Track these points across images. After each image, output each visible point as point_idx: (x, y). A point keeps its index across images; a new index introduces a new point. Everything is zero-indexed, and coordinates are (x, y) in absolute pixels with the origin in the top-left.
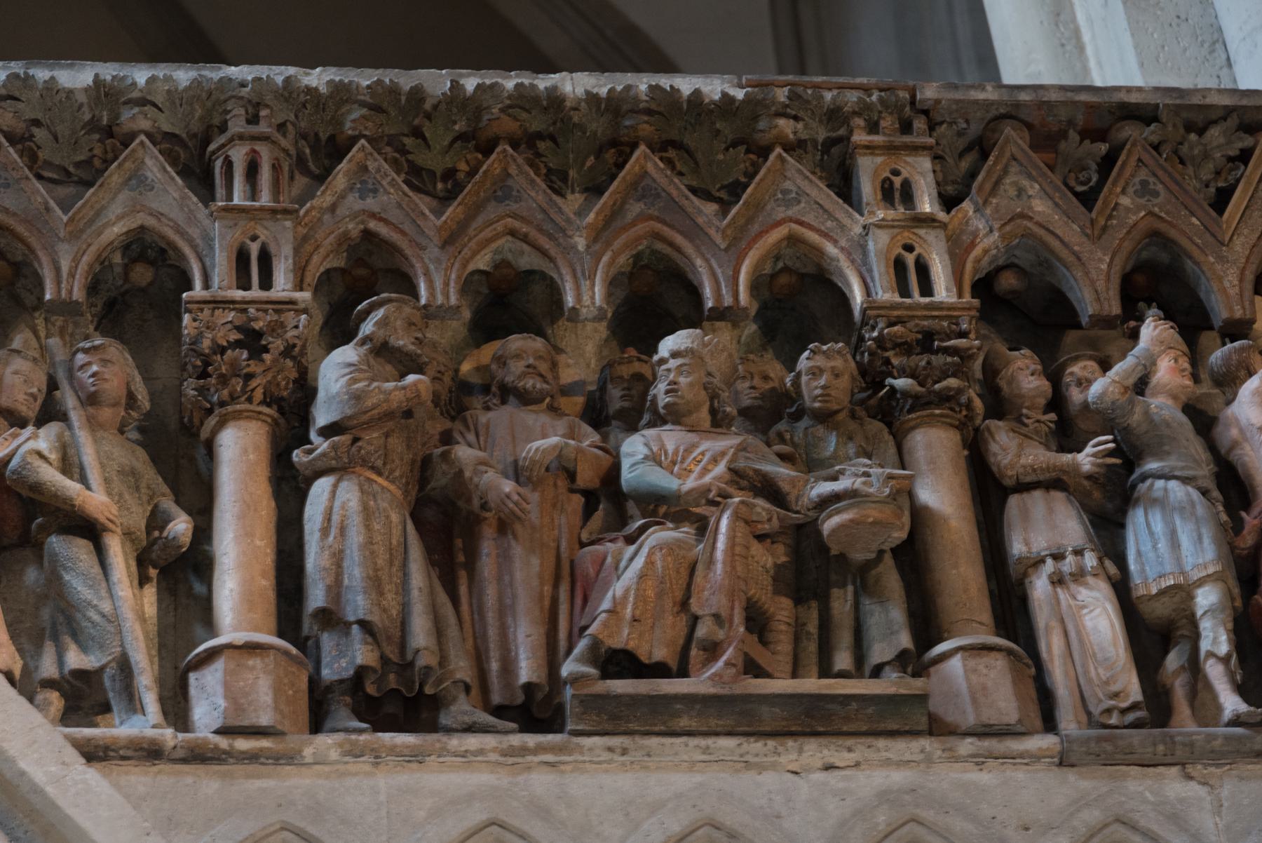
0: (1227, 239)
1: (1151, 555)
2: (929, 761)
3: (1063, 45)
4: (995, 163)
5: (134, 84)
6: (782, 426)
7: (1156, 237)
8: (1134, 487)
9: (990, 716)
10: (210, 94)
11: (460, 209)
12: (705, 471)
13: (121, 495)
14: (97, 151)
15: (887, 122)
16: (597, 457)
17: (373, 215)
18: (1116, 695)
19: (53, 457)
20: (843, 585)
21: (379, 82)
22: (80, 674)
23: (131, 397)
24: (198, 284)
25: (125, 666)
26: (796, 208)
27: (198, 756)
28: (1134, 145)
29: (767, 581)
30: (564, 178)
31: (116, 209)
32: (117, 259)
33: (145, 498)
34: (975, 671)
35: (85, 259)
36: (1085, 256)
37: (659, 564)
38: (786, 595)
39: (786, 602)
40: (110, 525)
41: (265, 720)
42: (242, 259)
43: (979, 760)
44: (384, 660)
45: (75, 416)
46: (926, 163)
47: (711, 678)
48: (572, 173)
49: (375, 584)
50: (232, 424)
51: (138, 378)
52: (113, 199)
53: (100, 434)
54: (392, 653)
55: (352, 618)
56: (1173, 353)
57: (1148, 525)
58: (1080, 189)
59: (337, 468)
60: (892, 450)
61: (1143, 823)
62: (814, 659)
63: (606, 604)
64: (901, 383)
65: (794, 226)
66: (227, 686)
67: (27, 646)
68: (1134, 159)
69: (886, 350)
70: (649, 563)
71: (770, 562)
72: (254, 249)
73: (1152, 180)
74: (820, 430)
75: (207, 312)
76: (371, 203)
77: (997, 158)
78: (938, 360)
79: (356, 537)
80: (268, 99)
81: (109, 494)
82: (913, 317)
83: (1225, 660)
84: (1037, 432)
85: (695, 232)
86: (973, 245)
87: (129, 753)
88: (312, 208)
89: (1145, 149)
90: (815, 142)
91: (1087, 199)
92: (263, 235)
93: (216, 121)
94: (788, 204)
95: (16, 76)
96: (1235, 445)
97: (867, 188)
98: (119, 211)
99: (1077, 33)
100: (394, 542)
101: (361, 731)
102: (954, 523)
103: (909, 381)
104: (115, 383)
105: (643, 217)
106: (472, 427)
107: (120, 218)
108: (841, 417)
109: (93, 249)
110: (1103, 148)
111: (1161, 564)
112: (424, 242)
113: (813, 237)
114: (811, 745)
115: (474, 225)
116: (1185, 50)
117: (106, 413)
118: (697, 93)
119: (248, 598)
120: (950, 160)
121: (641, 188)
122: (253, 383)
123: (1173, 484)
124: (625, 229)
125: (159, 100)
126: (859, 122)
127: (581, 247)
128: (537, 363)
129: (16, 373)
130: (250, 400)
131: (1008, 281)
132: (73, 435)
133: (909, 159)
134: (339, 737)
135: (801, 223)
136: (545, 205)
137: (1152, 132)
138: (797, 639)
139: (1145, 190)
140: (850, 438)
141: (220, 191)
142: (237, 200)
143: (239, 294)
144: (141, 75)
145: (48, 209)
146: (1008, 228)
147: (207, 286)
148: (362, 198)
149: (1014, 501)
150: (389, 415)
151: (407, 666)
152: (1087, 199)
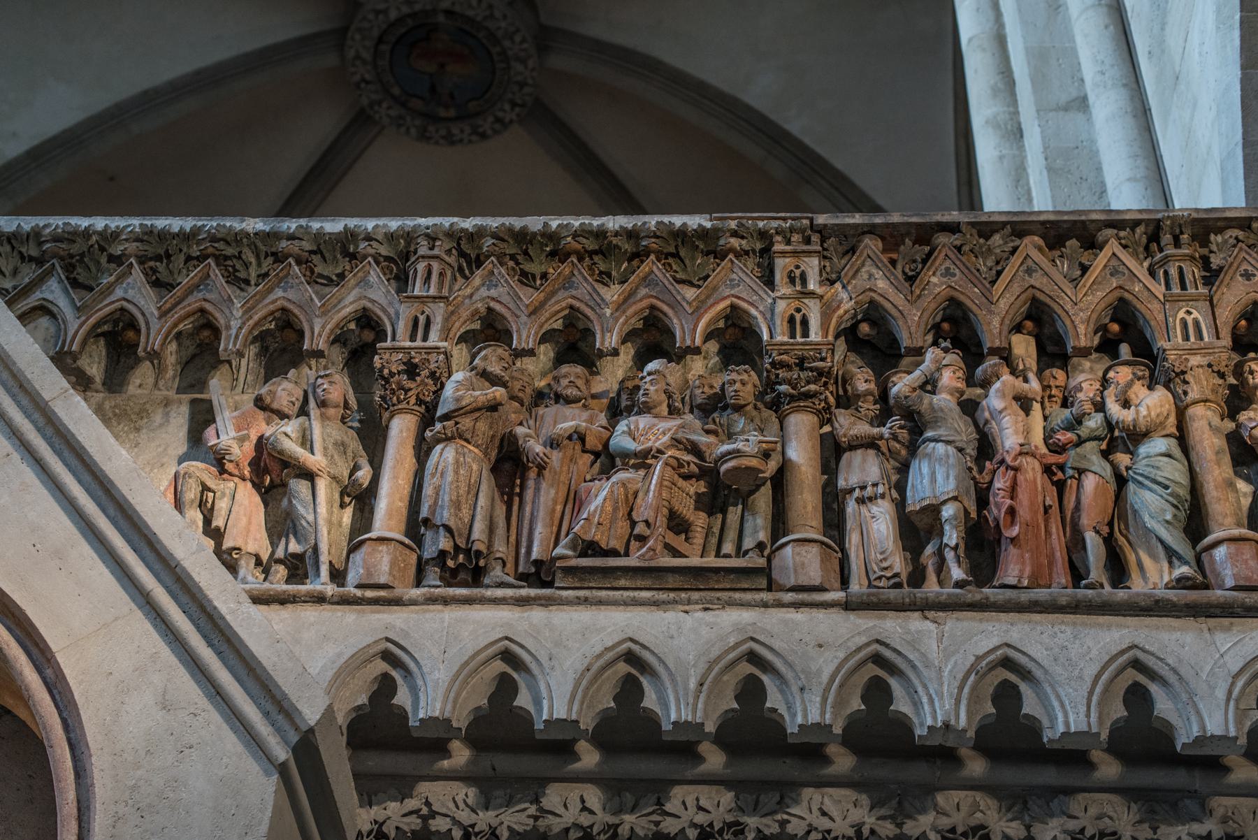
0: (995, 300)
1: (919, 486)
2: (765, 605)
3: (1019, 199)
4: (857, 260)
5: (366, 229)
6: (715, 415)
7: (953, 301)
9: (803, 581)
10: (408, 233)
11: (542, 294)
12: (658, 439)
13: (332, 457)
15: (796, 238)
16: (600, 432)
17: (493, 299)
18: (886, 569)
22: (294, 556)
23: (346, 402)
24: (389, 339)
26: (736, 289)
28: (944, 246)
29: (691, 503)
30: (609, 275)
31: (350, 298)
32: (352, 326)
33: (350, 458)
35: (329, 327)
36: (905, 313)
37: (616, 492)
39: (703, 515)
40: (321, 473)
41: (383, 580)
43: (797, 605)
44: (456, 547)
46: (815, 261)
48: (614, 273)
49: (457, 505)
51: (351, 391)
55: (439, 523)
56: (952, 368)
57: (920, 469)
58: (910, 274)
60: (776, 426)
61: (893, 644)
62: (714, 547)
64: (783, 388)
65: (733, 299)
68: (943, 254)
69: (778, 369)
71: (692, 491)
72: (422, 319)
73: (952, 267)
74: (736, 416)
75: (388, 355)
76: (493, 293)
78: (804, 375)
79: (450, 477)
81: (325, 455)
83: (956, 548)
84: (866, 415)
86: (839, 307)
87: (308, 599)
88: (459, 296)
89: (950, 249)
90: (754, 251)
91: (911, 279)
92: (427, 311)
93: (412, 249)
94: (733, 287)
95: (301, 226)
96: (987, 422)
97: (779, 276)
99: (1029, 192)
100: (472, 481)
102: (803, 469)
103: (787, 387)
104: (336, 394)
106: (533, 416)
107: (351, 303)
108: (749, 408)
110: (927, 249)
111: (924, 492)
112: (518, 313)
114: (695, 596)
116: (1083, 198)
117: (331, 411)
118: (684, 224)
119: (390, 514)
120: (835, 260)
122: (410, 394)
125: (380, 238)
126: (779, 238)
127: (608, 315)
128: (576, 381)
129: (284, 390)
130: (408, 403)
132: (310, 424)
133: (805, 259)
136: (591, 291)
137: (955, 239)
139: (948, 272)
140: (752, 421)
141: (410, 288)
142: (416, 293)
144: (370, 224)
145: (312, 299)
146: (860, 297)
147: (394, 339)
149: (846, 456)
151: (468, 551)
152: (911, 279)
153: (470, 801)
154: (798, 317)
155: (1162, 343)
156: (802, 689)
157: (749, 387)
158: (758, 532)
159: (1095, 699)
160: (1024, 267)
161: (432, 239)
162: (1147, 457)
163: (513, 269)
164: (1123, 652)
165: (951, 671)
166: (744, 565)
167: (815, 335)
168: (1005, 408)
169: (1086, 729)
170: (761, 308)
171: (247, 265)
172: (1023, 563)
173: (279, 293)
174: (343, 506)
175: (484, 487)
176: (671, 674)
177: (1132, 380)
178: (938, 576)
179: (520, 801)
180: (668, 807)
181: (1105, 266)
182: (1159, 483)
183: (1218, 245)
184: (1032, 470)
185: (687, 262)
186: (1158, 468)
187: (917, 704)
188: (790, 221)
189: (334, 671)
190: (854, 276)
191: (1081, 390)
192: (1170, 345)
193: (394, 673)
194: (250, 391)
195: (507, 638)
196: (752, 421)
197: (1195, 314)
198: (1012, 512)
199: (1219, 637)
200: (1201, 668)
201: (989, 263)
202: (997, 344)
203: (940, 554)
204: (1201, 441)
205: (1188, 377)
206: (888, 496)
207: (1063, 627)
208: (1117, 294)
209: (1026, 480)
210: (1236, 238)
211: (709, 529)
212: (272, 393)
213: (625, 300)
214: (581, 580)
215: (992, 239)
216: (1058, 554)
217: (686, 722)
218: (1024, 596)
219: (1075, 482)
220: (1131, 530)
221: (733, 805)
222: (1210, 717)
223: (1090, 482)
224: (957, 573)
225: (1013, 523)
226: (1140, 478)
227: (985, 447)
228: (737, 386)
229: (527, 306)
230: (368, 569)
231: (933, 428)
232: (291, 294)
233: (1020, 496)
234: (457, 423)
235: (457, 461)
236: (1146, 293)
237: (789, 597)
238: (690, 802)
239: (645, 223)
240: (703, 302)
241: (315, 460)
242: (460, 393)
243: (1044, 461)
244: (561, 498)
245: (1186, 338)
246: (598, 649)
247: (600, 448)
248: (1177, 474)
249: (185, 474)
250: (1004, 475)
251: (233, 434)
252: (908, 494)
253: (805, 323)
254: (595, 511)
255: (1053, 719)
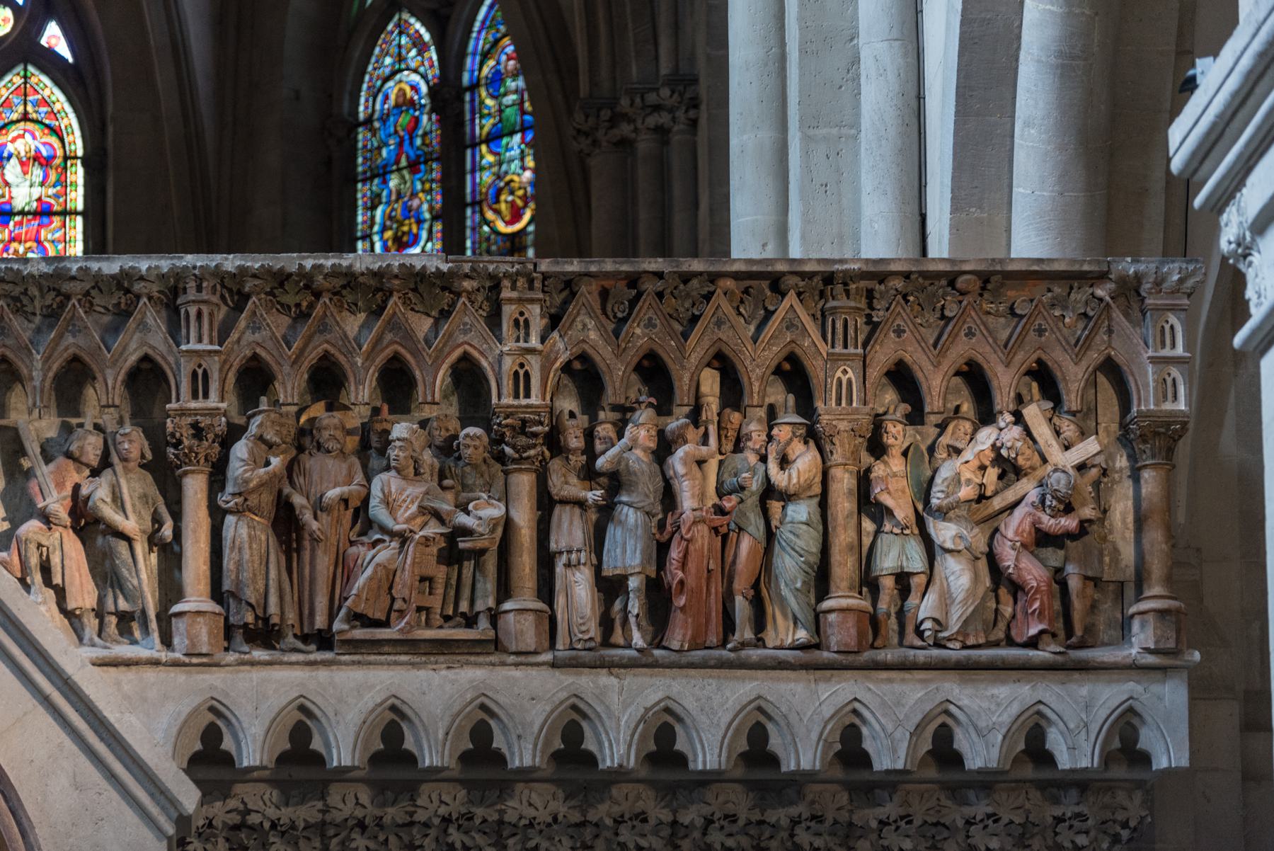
2: (493, 665)
7: (652, 350)
8: (616, 504)
9: (522, 648)
14: (123, 300)
16: (359, 492)
17: (258, 344)
18: (582, 632)
19: (109, 500)
20: (469, 560)
21: (262, 266)
23: (143, 456)
24: (174, 399)
25: (144, 612)
27: (176, 664)
28: (648, 294)
30: (356, 305)
31: (133, 345)
34: (519, 622)
35: (120, 378)
36: (612, 367)
38: (443, 564)
39: (443, 568)
41: (204, 650)
42: (195, 374)
43: (517, 665)
44: (257, 617)
45: (119, 467)
46: (536, 309)
47: (399, 631)
50: (190, 475)
52: (131, 338)
53: (132, 475)
54: (260, 614)
58: (620, 315)
59: (236, 512)
61: (586, 699)
63: (354, 591)
64: (508, 450)
66: (188, 631)
67: (99, 583)
68: (647, 303)
70: (375, 572)
72: (200, 372)
73: (655, 317)
74: (468, 469)
77: (575, 306)
80: (207, 276)
82: (517, 412)
83: (637, 616)
84: (575, 468)
85: (416, 353)
86: (556, 359)
90: (484, 288)
94: (465, 332)
96: (671, 478)
98: (134, 347)
101: (245, 653)
102: (523, 531)
105: (392, 342)
109: (123, 371)
110: (634, 292)
113: (476, 354)
114: (441, 658)
115: (308, 350)
118: (424, 267)
121: (393, 325)
122: (200, 456)
123: (631, 510)
124: (382, 350)
125: (152, 279)
127: (359, 364)
130: (198, 462)
131: (577, 365)
133: (529, 307)
134: (237, 656)
135: (471, 345)
137: (660, 285)
138: (446, 587)
139: (650, 324)
143: (193, 405)
144: (143, 264)
145: (100, 348)
148: (253, 333)
150: (262, 485)
151: (266, 620)
153: (274, 800)
154: (521, 372)
155: (819, 404)
156: (519, 737)
157: (481, 449)
158: (487, 597)
159: (726, 741)
160: (714, 319)
161: (199, 280)
162: (792, 522)
163: (271, 301)
164: (751, 702)
165: (626, 722)
166: (478, 637)
167: (534, 400)
168: (686, 474)
169: (716, 767)
170: (490, 359)
171: (32, 300)
172: (686, 628)
173: (69, 340)
174: (151, 550)
175: (272, 558)
176: (424, 725)
177: (791, 439)
178: (623, 629)
179: (310, 799)
180: (419, 802)
181: (783, 319)
182: (797, 552)
183: (881, 293)
184: (702, 536)
185: (425, 295)
186: (797, 536)
187: (600, 743)
188: (517, 266)
189: (178, 727)
190: (570, 327)
191: (750, 439)
192: (826, 408)
193: (219, 723)
194: (47, 417)
195: (302, 696)
196: (482, 476)
197: (850, 374)
198: (681, 582)
199: (822, 686)
200: (805, 714)
201: (687, 305)
202: (686, 401)
203: (625, 609)
204: (836, 506)
205: (835, 440)
206: (589, 562)
207: (711, 681)
208: (788, 349)
209: (695, 550)
210: (896, 290)
211: (448, 579)
212: (81, 448)
213: (373, 348)
214: (354, 648)
215: (691, 283)
216: (714, 614)
217: (437, 767)
218: (685, 659)
219: (736, 535)
220: (772, 585)
221: (466, 799)
222: (804, 755)
223: (746, 544)
224: (638, 639)
225: (681, 591)
226: (784, 544)
227: (669, 497)
228: (469, 451)
229: (290, 357)
230: (191, 640)
231: (629, 492)
232: (81, 340)
233: (690, 565)
234: (246, 500)
235: (250, 536)
236: (813, 349)
237: (512, 659)
238: (435, 797)
239: (389, 265)
240: (441, 350)
241: (130, 524)
242: (247, 475)
243: (712, 525)
244: (333, 561)
245: (839, 402)
246: (371, 705)
247: (359, 504)
248: (811, 542)
249: (26, 540)
250: (679, 544)
251: (55, 494)
252: (605, 558)
253: (527, 375)
254: (363, 588)
255: (695, 755)
